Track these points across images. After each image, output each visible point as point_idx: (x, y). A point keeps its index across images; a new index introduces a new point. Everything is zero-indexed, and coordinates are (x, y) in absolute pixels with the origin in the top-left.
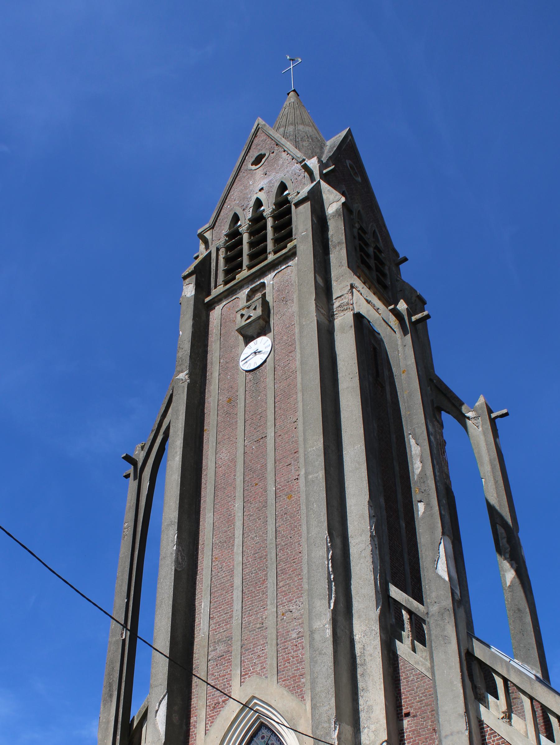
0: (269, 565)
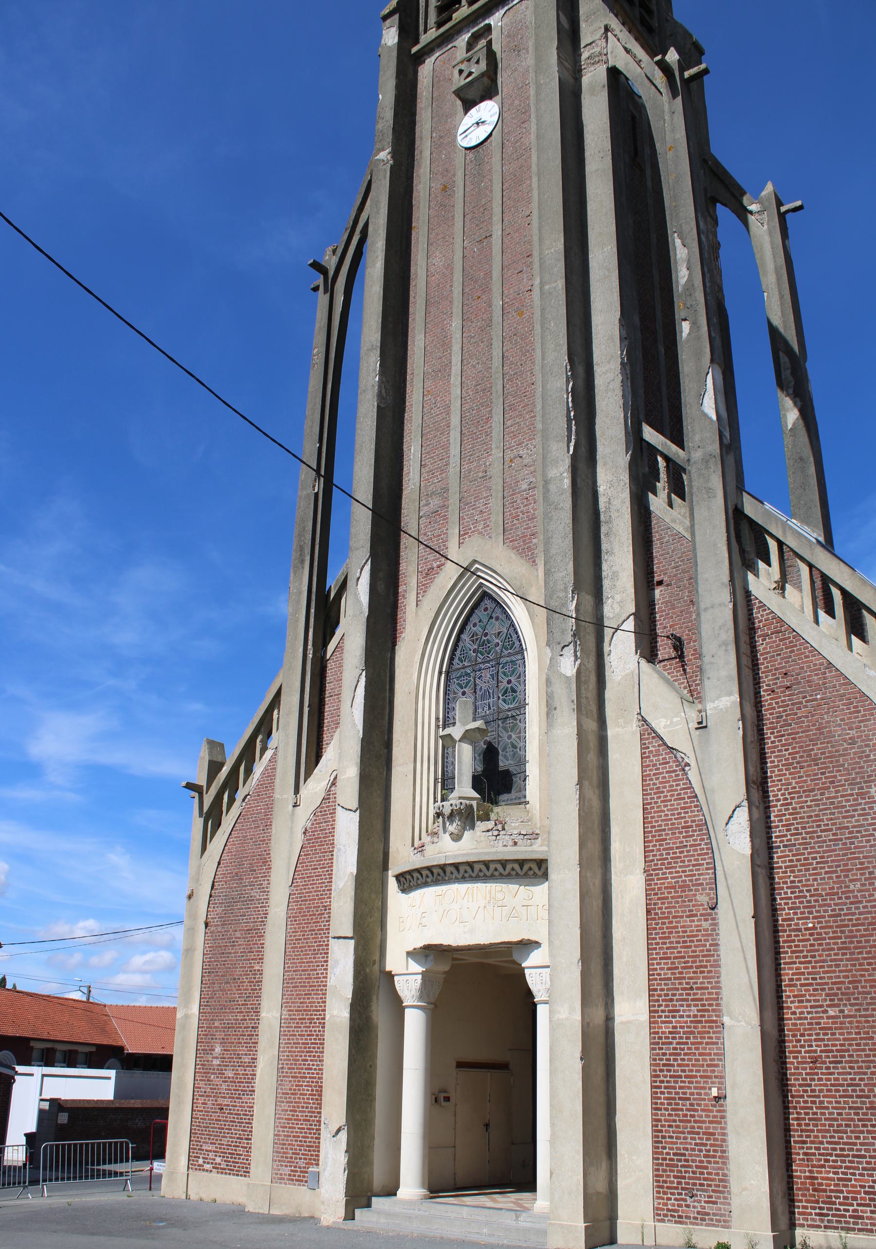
0: (494, 400)
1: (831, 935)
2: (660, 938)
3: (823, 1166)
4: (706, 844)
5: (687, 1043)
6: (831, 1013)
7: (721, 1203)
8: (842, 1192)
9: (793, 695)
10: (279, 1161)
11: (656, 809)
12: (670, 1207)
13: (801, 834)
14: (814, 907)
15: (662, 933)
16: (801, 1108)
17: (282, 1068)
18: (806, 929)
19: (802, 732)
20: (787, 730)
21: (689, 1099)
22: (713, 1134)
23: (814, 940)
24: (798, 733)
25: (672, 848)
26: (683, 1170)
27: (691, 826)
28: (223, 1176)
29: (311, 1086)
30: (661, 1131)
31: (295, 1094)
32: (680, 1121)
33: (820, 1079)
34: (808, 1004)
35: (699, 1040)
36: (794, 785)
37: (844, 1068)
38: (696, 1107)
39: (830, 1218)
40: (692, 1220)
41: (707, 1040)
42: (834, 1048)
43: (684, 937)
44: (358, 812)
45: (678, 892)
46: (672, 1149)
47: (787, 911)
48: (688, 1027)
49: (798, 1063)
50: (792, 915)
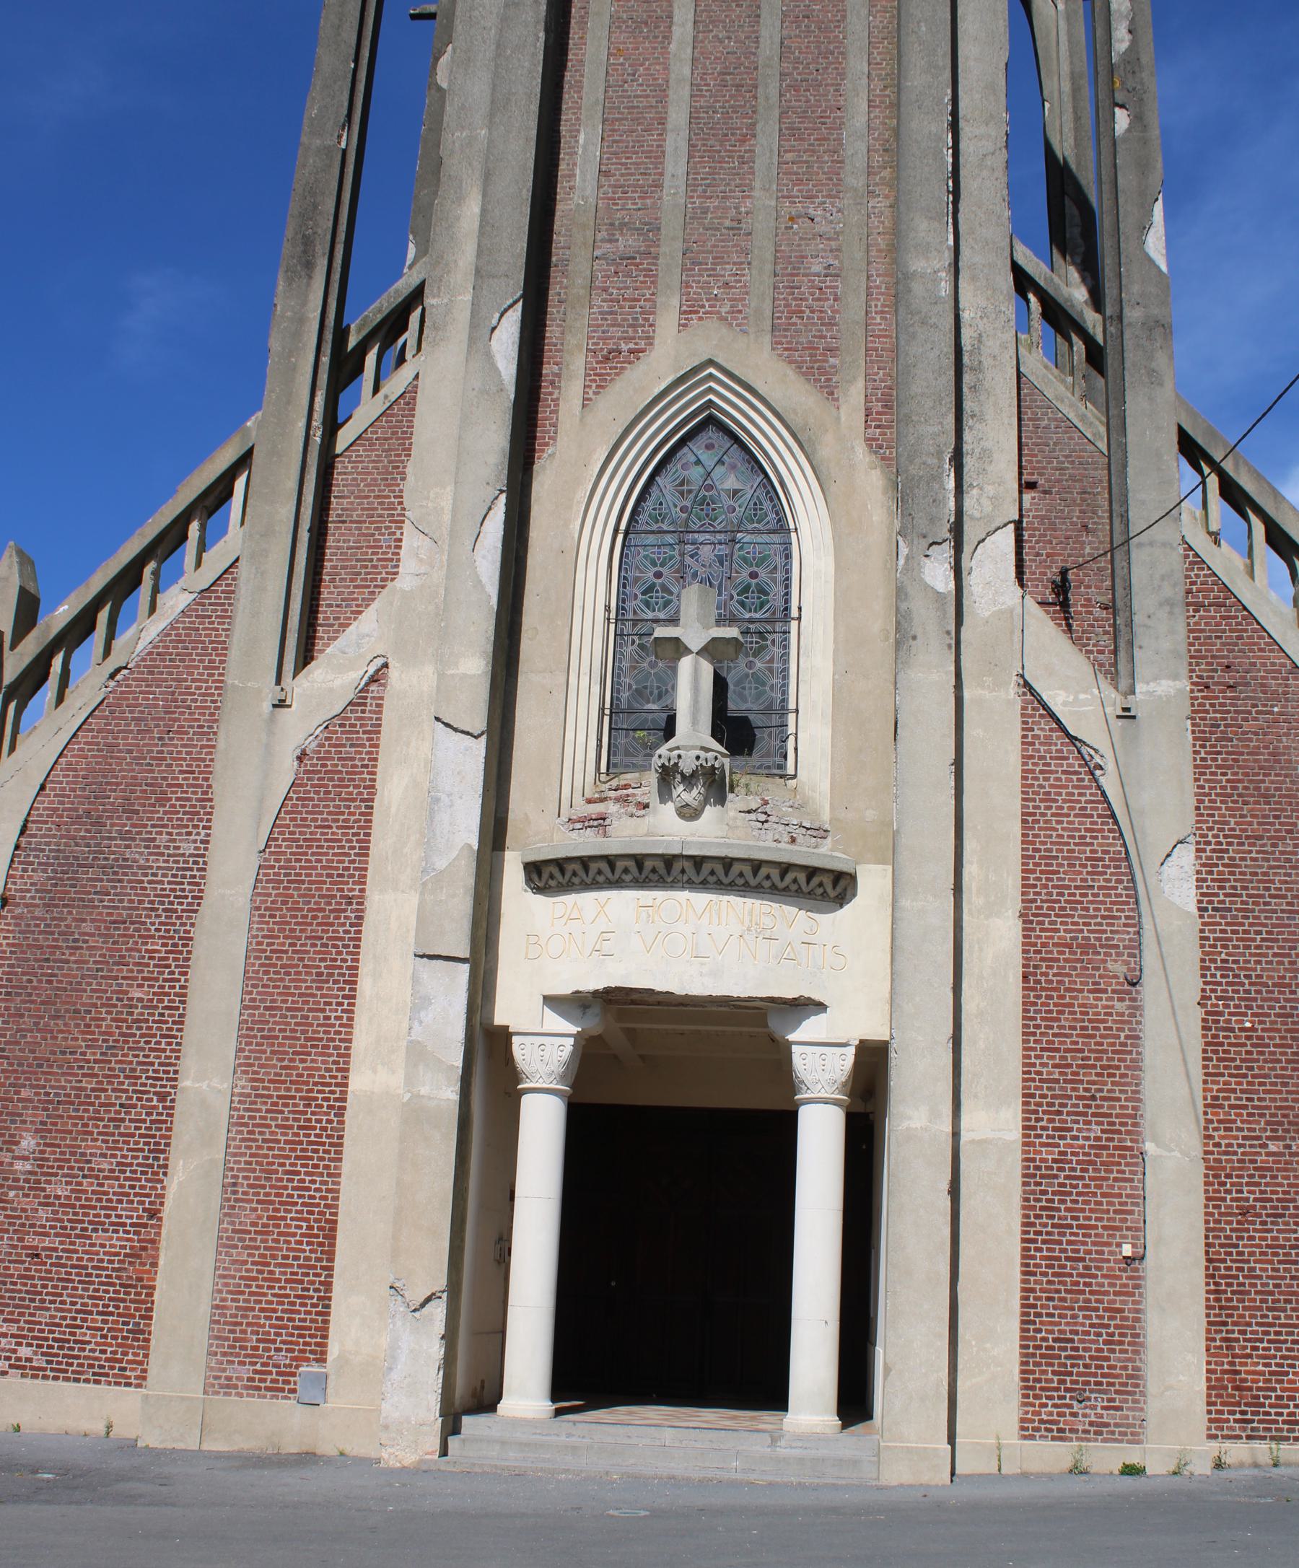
0: (761, 109)
1: (1277, 1041)
2: (1042, 1019)
3: (1250, 1356)
4: (1126, 888)
5: (1083, 1178)
6: (1272, 1147)
7: (1128, 1409)
8: (1274, 1390)
9: (1238, 698)
10: (224, 1354)
11: (1041, 824)
12: (1044, 1417)
13: (1241, 896)
14: (1255, 999)
15: (1046, 1012)
16: (1222, 1277)
17: (234, 1185)
18: (1241, 1029)
19: (1248, 754)
20: (1226, 746)
21: (1083, 1259)
22: (1121, 1311)
23: (1253, 1045)
24: (1242, 754)
25: (1068, 887)
26: (1069, 1362)
27: (1102, 859)
28: (39, 1382)
29: (307, 1220)
30: (1035, 1306)
31: (267, 1233)
32: (1066, 1291)
33: (1251, 1238)
34: (1240, 1134)
35: (1103, 1174)
36: (1232, 825)
37: (1287, 1224)
38: (1093, 1271)
39: (1255, 1425)
40: (1080, 1435)
41: (1115, 1175)
42: (1274, 1197)
43: (1083, 1021)
44: (484, 737)
45: (1075, 953)
46: (1052, 1332)
47: (1214, 1001)
48: (1084, 1154)
49: (1220, 1214)
50: (1221, 1008)
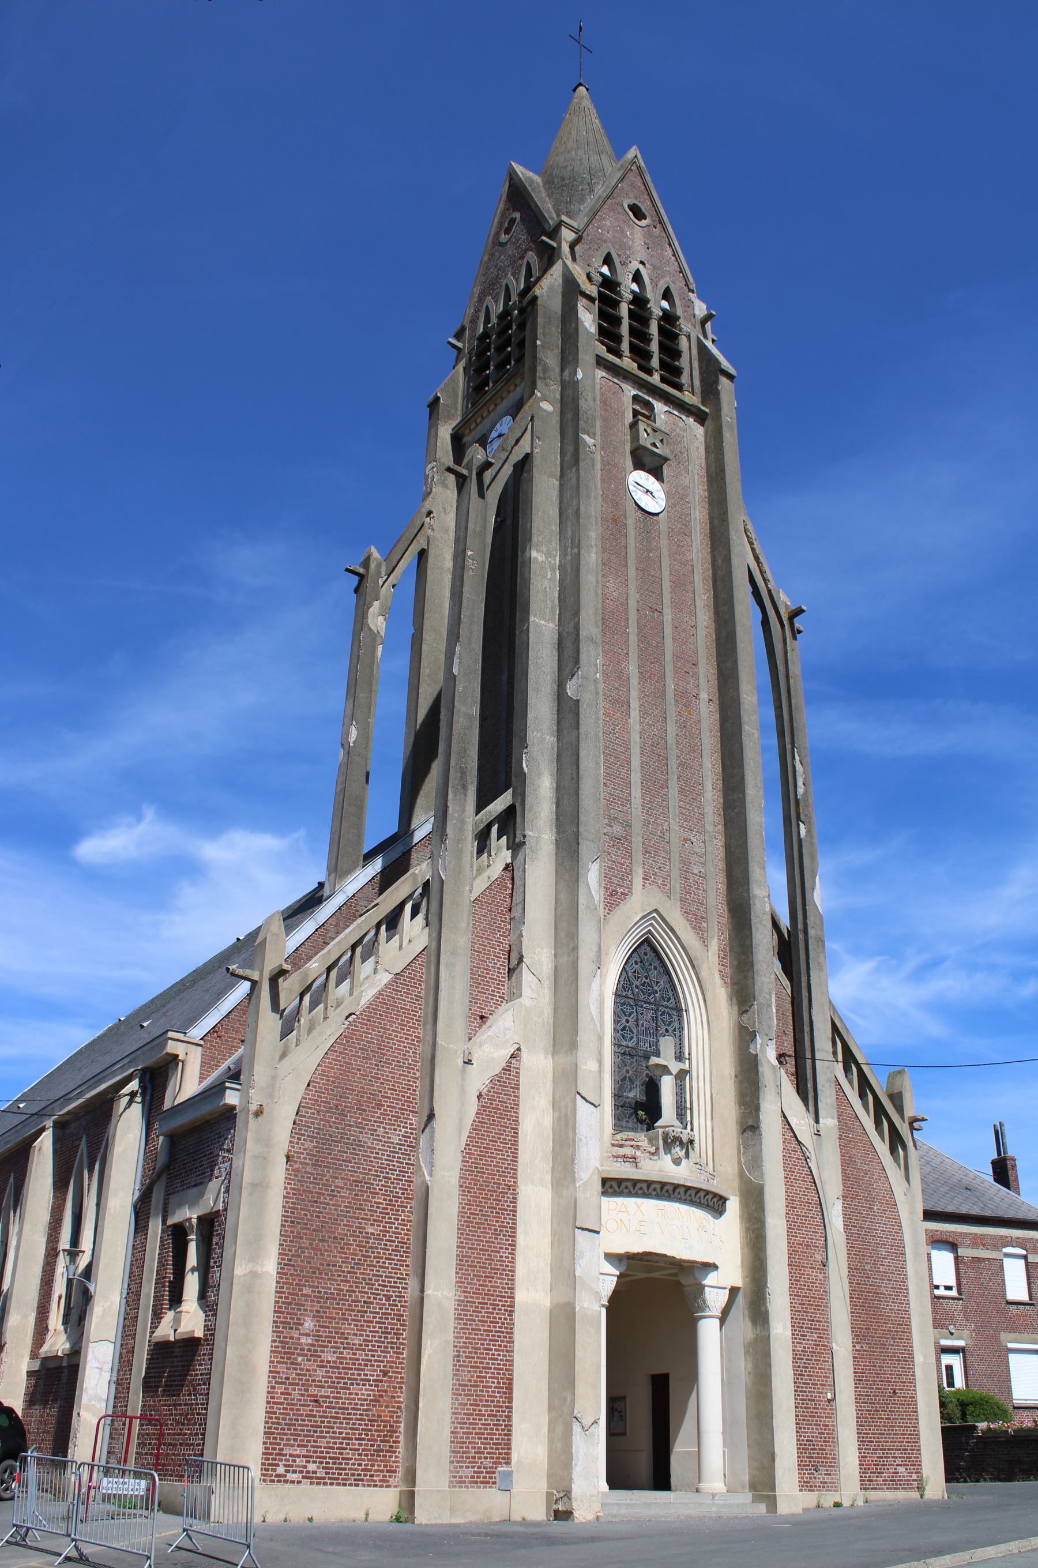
10: (458, 1462)
17: (458, 1356)
28: (321, 1487)
29: (497, 1378)
31: (477, 1386)
